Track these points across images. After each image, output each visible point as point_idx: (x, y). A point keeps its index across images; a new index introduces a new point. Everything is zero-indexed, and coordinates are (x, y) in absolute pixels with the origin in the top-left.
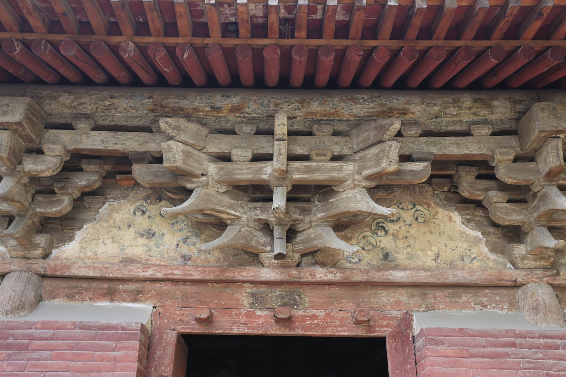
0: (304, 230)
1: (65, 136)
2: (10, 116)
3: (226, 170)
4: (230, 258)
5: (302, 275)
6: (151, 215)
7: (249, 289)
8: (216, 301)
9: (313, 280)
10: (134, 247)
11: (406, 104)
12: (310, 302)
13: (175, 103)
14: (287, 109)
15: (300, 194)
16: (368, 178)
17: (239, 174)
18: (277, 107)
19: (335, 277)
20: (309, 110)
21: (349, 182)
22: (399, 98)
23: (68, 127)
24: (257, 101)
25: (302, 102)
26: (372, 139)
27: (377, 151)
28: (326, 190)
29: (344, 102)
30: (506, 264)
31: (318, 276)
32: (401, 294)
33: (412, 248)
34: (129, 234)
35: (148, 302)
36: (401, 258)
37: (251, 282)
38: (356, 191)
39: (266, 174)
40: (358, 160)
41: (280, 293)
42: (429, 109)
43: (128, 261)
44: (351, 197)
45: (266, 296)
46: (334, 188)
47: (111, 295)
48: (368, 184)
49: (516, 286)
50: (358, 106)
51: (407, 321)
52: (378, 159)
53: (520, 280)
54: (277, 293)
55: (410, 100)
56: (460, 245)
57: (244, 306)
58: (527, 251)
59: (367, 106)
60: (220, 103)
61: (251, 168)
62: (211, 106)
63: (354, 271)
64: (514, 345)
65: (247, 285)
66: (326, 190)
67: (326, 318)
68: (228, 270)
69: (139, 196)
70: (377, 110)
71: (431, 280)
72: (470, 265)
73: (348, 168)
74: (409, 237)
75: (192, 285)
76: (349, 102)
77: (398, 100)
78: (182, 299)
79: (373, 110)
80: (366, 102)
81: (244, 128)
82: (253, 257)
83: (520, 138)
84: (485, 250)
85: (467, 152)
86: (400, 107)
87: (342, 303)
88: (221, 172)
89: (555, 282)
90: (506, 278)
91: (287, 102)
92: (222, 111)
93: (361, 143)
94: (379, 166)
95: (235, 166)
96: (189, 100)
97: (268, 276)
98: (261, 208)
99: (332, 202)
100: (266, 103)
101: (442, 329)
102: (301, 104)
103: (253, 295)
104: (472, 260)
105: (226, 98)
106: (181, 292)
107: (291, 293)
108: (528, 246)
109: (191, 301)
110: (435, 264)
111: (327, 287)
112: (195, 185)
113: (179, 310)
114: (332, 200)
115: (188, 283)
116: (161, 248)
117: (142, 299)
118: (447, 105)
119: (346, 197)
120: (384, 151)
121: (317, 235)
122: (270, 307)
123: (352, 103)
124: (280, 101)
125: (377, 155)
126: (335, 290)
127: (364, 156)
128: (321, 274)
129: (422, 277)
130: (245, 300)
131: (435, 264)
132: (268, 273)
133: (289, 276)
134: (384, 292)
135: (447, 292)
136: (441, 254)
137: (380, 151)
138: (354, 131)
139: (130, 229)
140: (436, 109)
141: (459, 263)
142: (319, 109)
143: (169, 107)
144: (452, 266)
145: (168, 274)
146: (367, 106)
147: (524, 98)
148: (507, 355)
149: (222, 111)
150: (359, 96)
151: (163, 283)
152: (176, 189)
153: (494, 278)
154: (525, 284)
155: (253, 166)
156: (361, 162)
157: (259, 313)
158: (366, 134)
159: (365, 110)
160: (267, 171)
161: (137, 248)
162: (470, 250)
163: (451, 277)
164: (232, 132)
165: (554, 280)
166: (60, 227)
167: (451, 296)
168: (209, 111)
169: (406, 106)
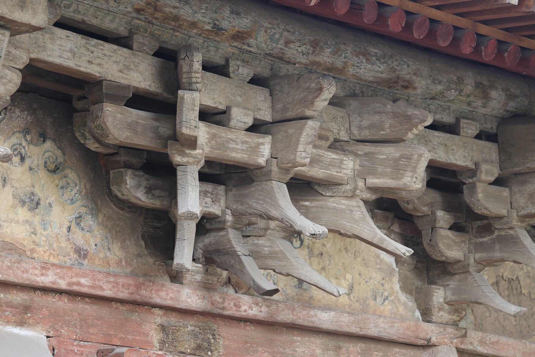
0: (249, 236)
2: (30, 11)
3: (218, 140)
5: (226, 304)
6: (33, 166)
8: (122, 335)
10: (13, 225)
11: (415, 74)
13: (174, 7)
14: (295, 51)
17: (233, 150)
18: (286, 46)
19: (261, 311)
20: (317, 59)
21: (348, 187)
22: (410, 63)
24: (269, 31)
26: (388, 131)
27: (397, 155)
29: (357, 56)
30: (415, 311)
31: (243, 308)
32: (316, 344)
33: (327, 271)
35: (39, 328)
38: (354, 203)
39: (263, 156)
40: (360, 155)
41: (193, 328)
42: (432, 87)
44: (342, 210)
45: (178, 331)
46: (316, 187)
48: (368, 196)
50: (369, 66)
52: (397, 167)
53: (434, 340)
54: (190, 328)
55: (419, 69)
56: (374, 275)
57: (154, 346)
58: (445, 299)
59: (376, 68)
60: (227, 22)
61: (245, 142)
62: (215, 24)
63: (280, 305)
65: (157, 311)
69: (14, 124)
70: (384, 75)
72: (382, 308)
74: (325, 255)
75: (92, 303)
76: (361, 57)
77: (408, 66)
78: (81, 326)
79: (380, 75)
80: (378, 62)
81: (240, 70)
83: (501, 151)
85: (454, 161)
86: (408, 77)
87: (257, 351)
88: (213, 142)
89: (462, 347)
90: (421, 336)
91: (299, 40)
92: (224, 34)
93: (366, 128)
94: (398, 179)
95: (230, 136)
96: (191, 8)
97: (189, 300)
98: (212, 194)
99: (306, 206)
100: (277, 36)
102: (314, 48)
104: (384, 301)
105: (235, 16)
106: (79, 314)
107: (204, 329)
109: (91, 331)
110: (348, 302)
111: (242, 324)
112: (185, 160)
113: (78, 345)
114: (307, 203)
115: (87, 299)
116: (49, 231)
117: (31, 321)
118: (451, 85)
119: (334, 208)
120: (410, 159)
121: (275, 253)
122: (183, 350)
123: (364, 61)
127: (374, 153)
130: (154, 335)
131: (348, 302)
133: (213, 304)
134: (299, 338)
136: (355, 286)
139: (6, 188)
142: (329, 60)
143: (164, 12)
145: (73, 284)
146: (376, 68)
147: (518, 92)
149: (224, 34)
150: (373, 50)
151: (57, 296)
153: (410, 334)
154: (435, 346)
155: (250, 140)
156: (367, 161)
159: (373, 74)
162: (382, 285)
165: (462, 343)
168: (208, 30)
169: (414, 78)
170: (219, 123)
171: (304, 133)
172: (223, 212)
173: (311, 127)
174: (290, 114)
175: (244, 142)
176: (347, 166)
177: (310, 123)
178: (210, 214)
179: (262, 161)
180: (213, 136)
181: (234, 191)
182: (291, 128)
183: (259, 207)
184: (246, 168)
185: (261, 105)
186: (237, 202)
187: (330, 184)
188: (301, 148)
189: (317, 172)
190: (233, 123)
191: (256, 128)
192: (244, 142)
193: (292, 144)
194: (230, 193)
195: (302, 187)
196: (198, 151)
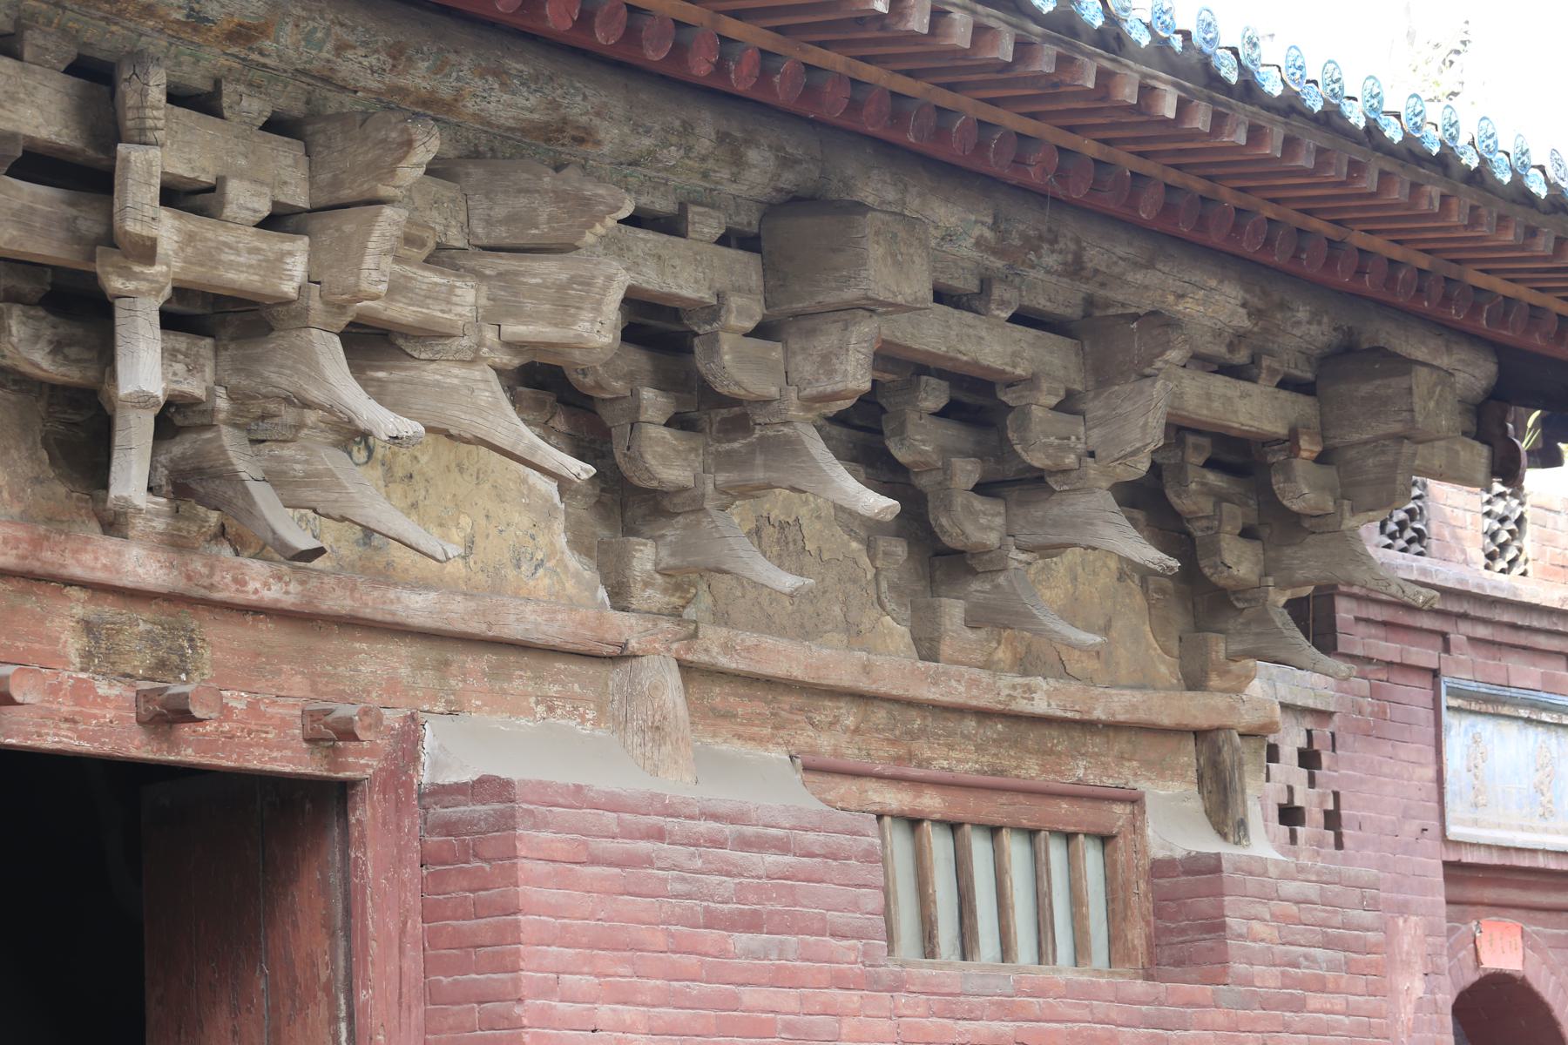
3: (199, 245)
4: (23, 490)
5: (216, 579)
7: (79, 606)
9: (239, 598)
11: (598, 114)
12: (215, 664)
16: (512, 346)
17: (231, 265)
18: (338, 56)
19: (287, 593)
20: (402, 82)
21: (465, 342)
24: (303, 25)
25: (396, 52)
26: (545, 228)
27: (564, 277)
29: (482, 77)
31: (251, 586)
32: (399, 656)
37: (84, 585)
38: (477, 374)
39: (291, 278)
40: (489, 277)
41: (149, 627)
42: (632, 140)
44: (454, 388)
45: (119, 632)
46: (400, 342)
49: (621, 656)
50: (505, 97)
51: (408, 742)
52: (564, 303)
53: (634, 644)
54: (143, 627)
55: (605, 105)
56: (516, 518)
58: (656, 564)
59: (521, 101)
61: (257, 251)
62: (192, 9)
63: (326, 580)
64: (659, 835)
68: (48, 539)
70: (536, 116)
71: (476, 627)
72: (532, 583)
73: (467, 298)
74: (416, 477)
79: (528, 115)
81: (244, 103)
83: (768, 269)
84: (562, 541)
85: (675, 290)
86: (584, 119)
87: (280, 672)
88: (189, 250)
89: (689, 657)
90: (609, 637)
91: (365, 44)
92: (210, 30)
94: (566, 325)
97: (141, 571)
98: (186, 355)
99: (379, 380)
100: (319, 35)
101: (542, 785)
102: (394, 58)
103: (88, 627)
108: (664, 553)
111: (249, 618)
112: (131, 285)
114: (381, 374)
119: (437, 384)
121: (318, 475)
122: (129, 670)
123: (496, 86)
124: (351, 39)
125: (562, 288)
126: (269, 634)
127: (517, 274)
133: (189, 578)
134: (364, 646)
135: (487, 659)
136: (477, 539)
137: (573, 280)
138: (476, 172)
140: (647, 142)
141: (511, 573)
142: (425, 84)
146: (521, 101)
147: (798, 153)
148: (648, 861)
149: (210, 30)
150: (514, 65)
153: (588, 634)
154: (635, 656)
155: (264, 246)
157: (103, 688)
158: (522, 202)
159: (513, 112)
162: (533, 537)
165: (688, 650)
167: (495, 674)
168: (178, 22)
169: (597, 121)
170: (200, 211)
171: (377, 233)
172: (211, 393)
173: (390, 220)
174: (346, 194)
175: (253, 251)
176: (462, 300)
177: (388, 211)
178: (182, 395)
179: (289, 289)
180: (190, 238)
181: (232, 350)
182: (348, 222)
183: (284, 382)
184: (256, 303)
185: (286, 175)
186: (237, 371)
187: (429, 336)
188: (369, 262)
189: (402, 312)
190: (229, 211)
191: (278, 220)
192: (253, 251)
193: (351, 253)
194: (224, 354)
195: (370, 342)
196: (158, 269)
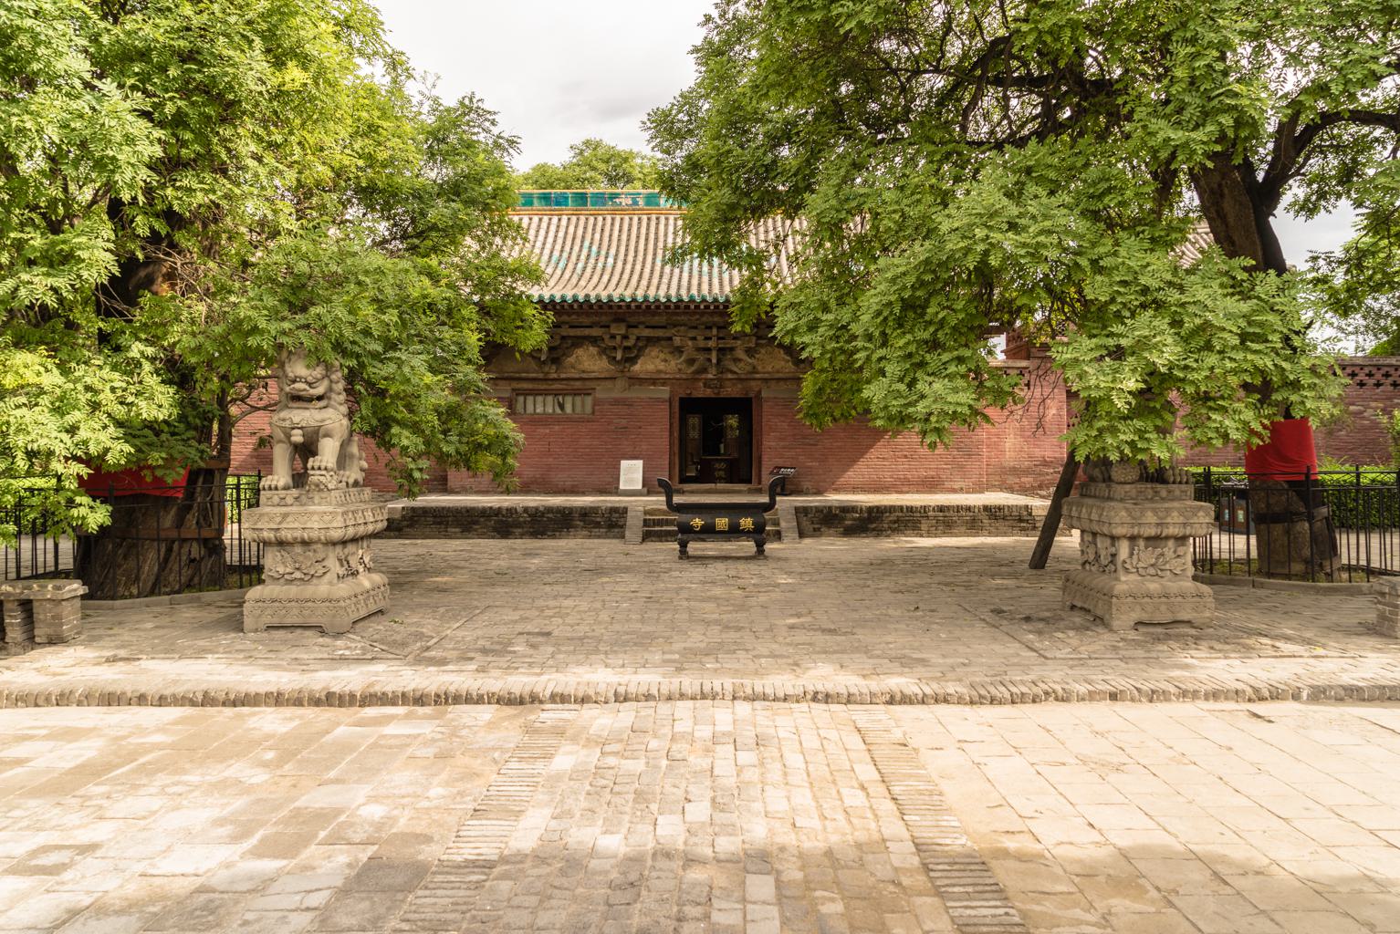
1: (635, 331)
15: (721, 351)
23: (635, 327)
28: (732, 349)
34: (657, 361)
36: (760, 368)
43: (659, 372)
47: (654, 384)
51: (760, 392)
66: (732, 349)
67: (731, 391)
82: (705, 370)
128: (730, 376)
129: (766, 376)
132: (710, 376)
144: (778, 372)
152: (678, 351)
160: (711, 344)
161: (662, 366)
163: (777, 376)
164: (696, 328)
166: (633, 361)
